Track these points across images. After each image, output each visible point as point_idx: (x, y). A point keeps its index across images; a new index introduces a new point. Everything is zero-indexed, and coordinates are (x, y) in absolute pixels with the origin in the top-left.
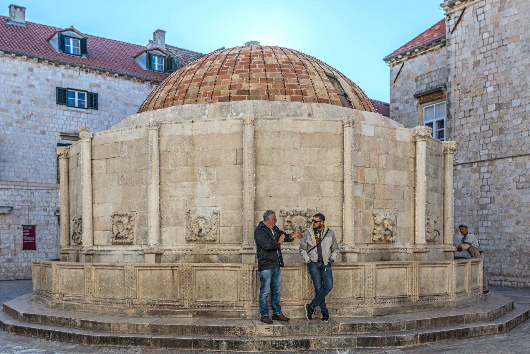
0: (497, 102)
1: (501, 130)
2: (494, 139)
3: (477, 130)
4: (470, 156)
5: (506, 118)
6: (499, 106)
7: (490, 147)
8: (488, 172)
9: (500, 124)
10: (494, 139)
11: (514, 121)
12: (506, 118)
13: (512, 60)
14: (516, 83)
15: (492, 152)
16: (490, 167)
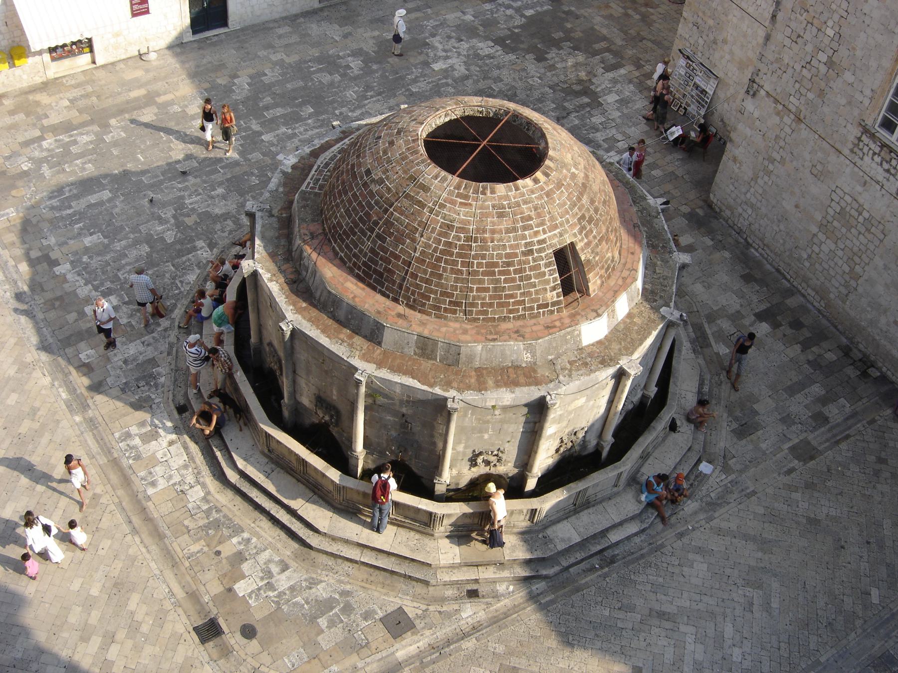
0: (830, 55)
1: (821, 94)
2: (810, 96)
3: (798, 67)
4: (779, 90)
5: (831, 84)
6: (830, 64)
7: (803, 100)
8: (790, 126)
9: (823, 84)
10: (810, 96)
11: (839, 96)
12: (831, 84)
13: (867, 21)
14: (859, 53)
15: (803, 108)
16: (794, 124)
